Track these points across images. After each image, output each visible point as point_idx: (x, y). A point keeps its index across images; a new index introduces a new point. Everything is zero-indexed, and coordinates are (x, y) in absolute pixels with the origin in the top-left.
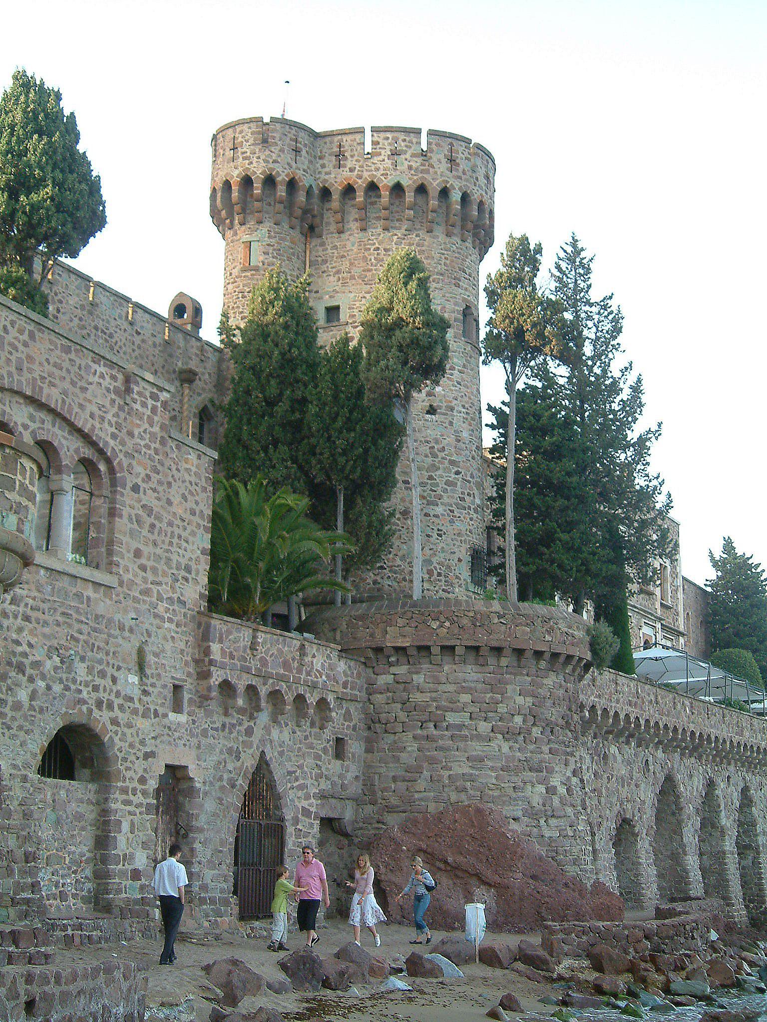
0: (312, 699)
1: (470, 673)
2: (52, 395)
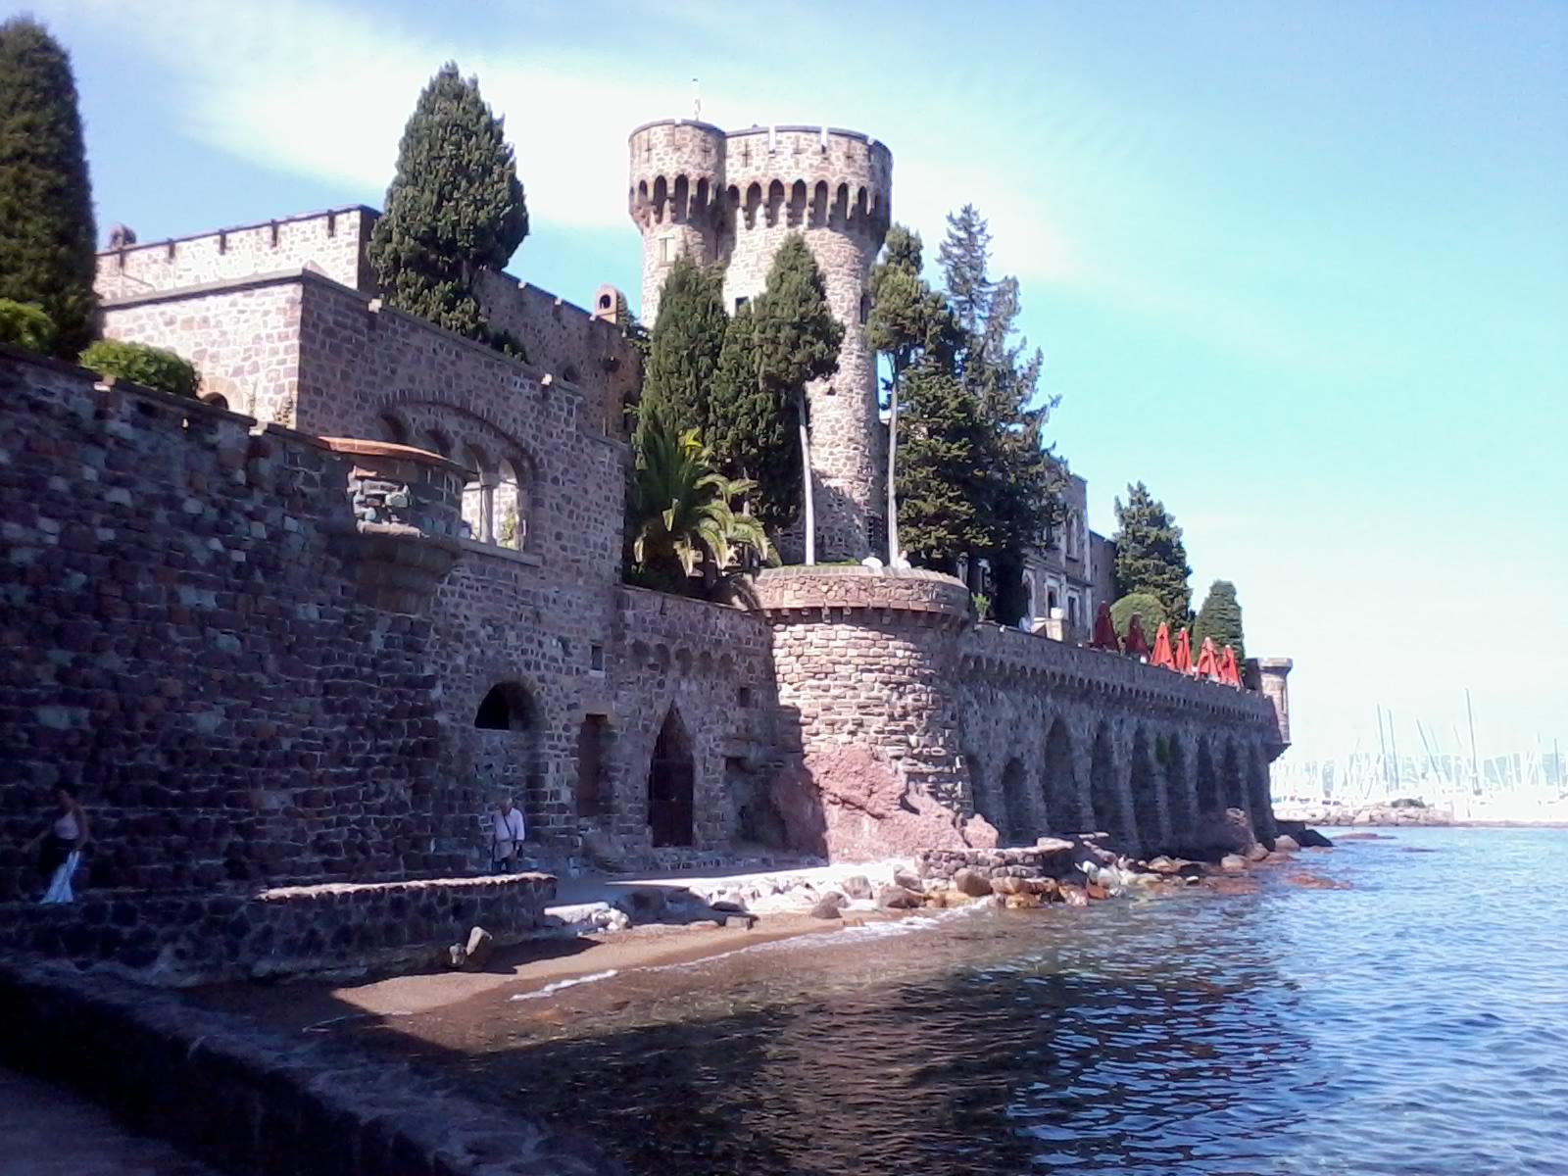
0: (716, 655)
2: (479, 405)
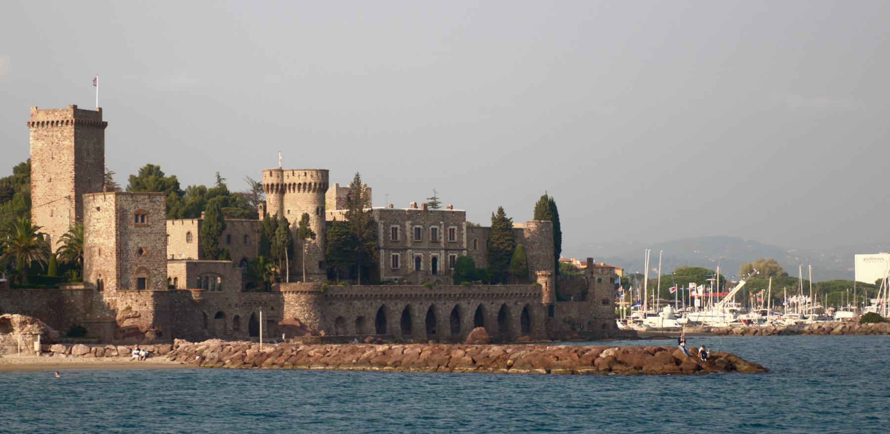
1: (295, 295)
2: (213, 271)
